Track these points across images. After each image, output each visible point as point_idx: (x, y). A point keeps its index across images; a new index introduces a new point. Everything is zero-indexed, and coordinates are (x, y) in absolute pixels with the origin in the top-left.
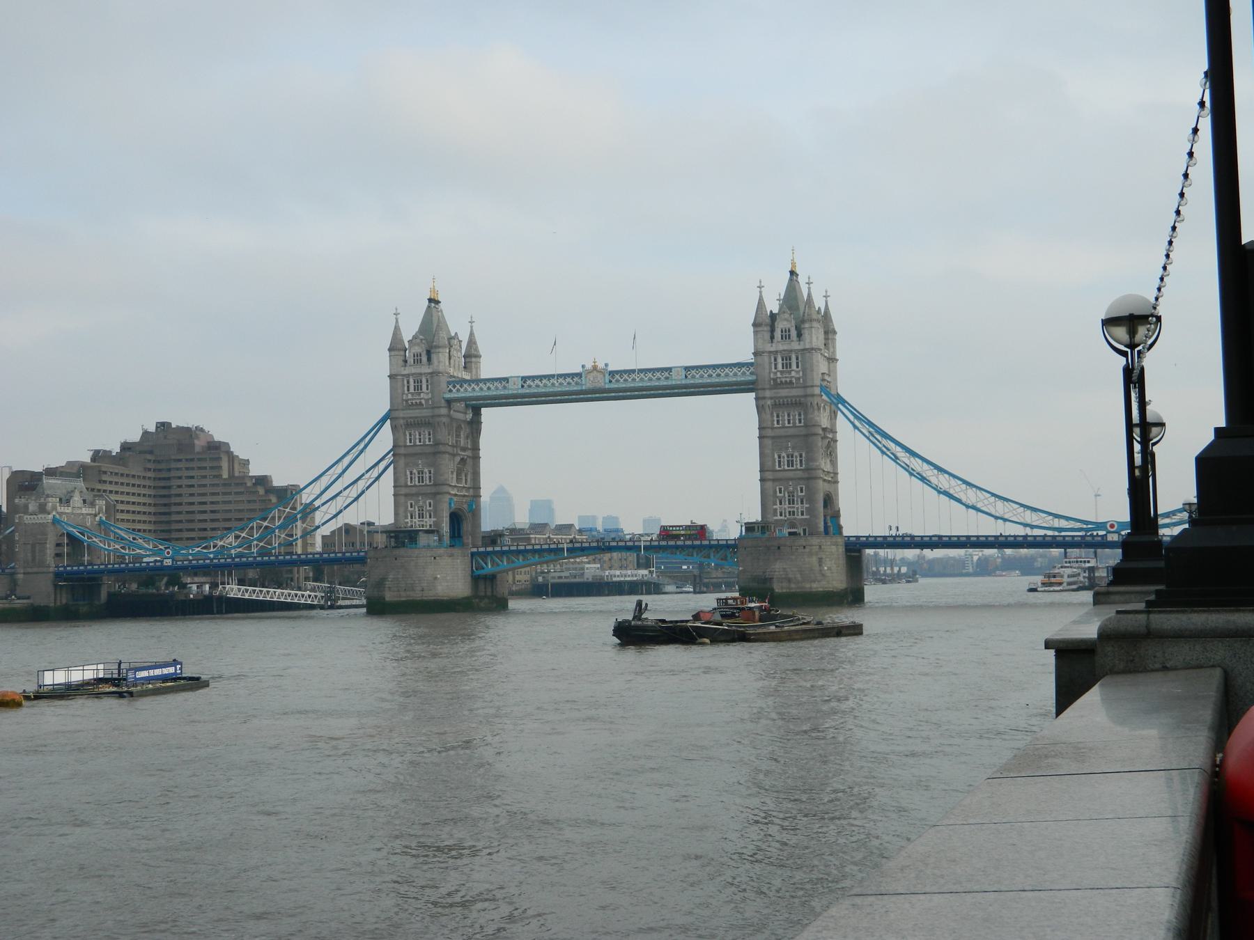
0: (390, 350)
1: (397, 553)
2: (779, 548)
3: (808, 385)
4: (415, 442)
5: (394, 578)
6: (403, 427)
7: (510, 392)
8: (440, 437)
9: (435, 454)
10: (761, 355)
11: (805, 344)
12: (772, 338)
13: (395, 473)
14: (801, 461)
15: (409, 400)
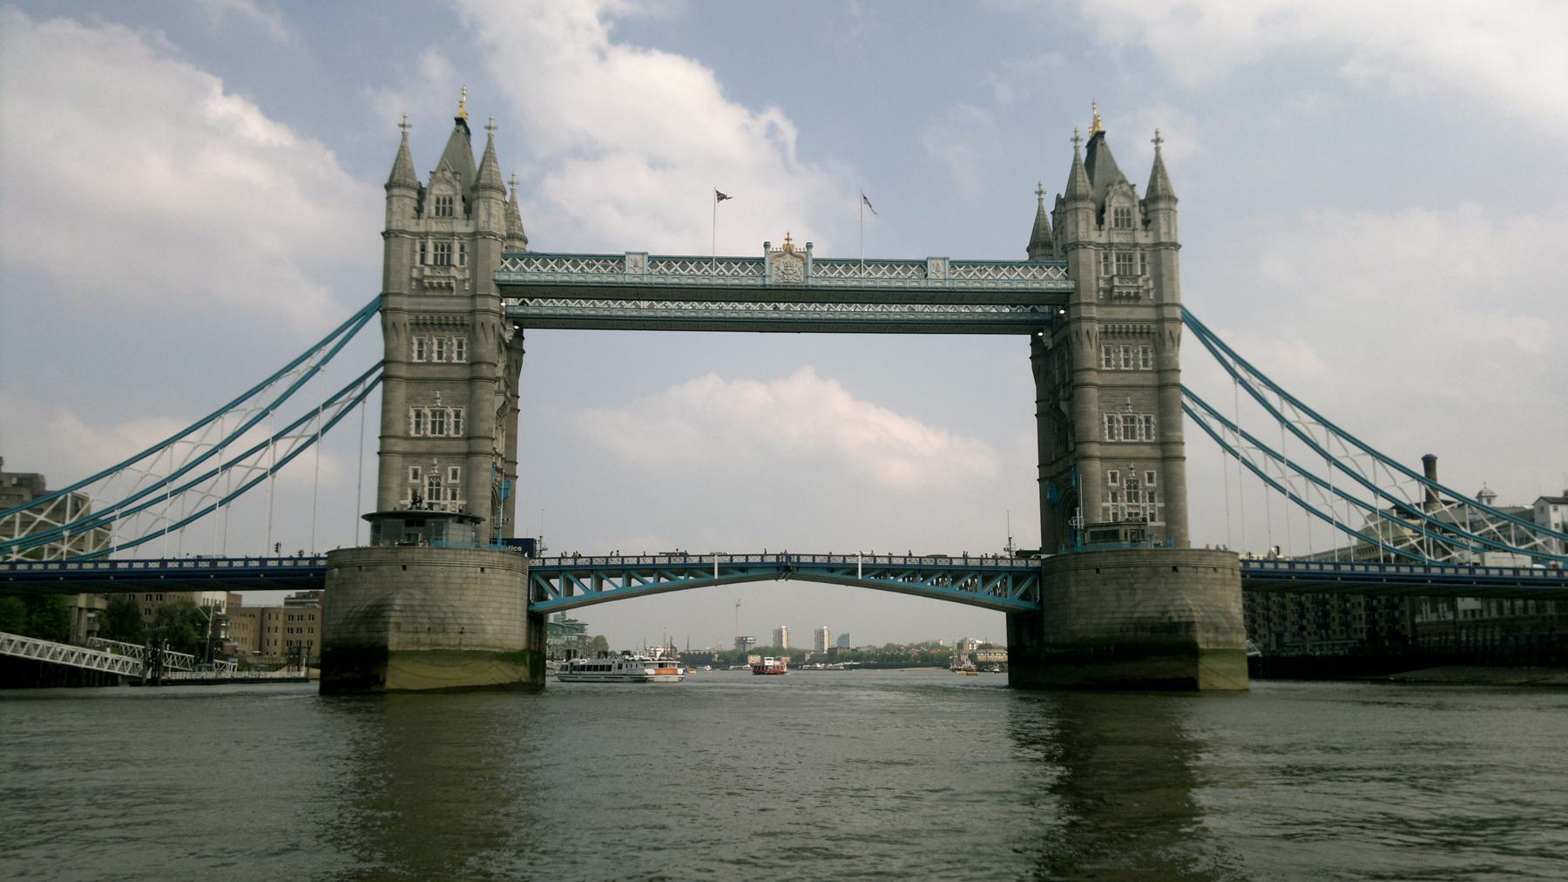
0: (388, 187)
1: (408, 555)
2: (1175, 569)
3: (1166, 301)
4: (430, 356)
5: (405, 606)
6: (408, 327)
7: (628, 279)
8: (484, 351)
9: (472, 380)
10: (1085, 248)
11: (1157, 234)
12: (1100, 221)
13: (385, 411)
14: (1148, 429)
15: (425, 277)
